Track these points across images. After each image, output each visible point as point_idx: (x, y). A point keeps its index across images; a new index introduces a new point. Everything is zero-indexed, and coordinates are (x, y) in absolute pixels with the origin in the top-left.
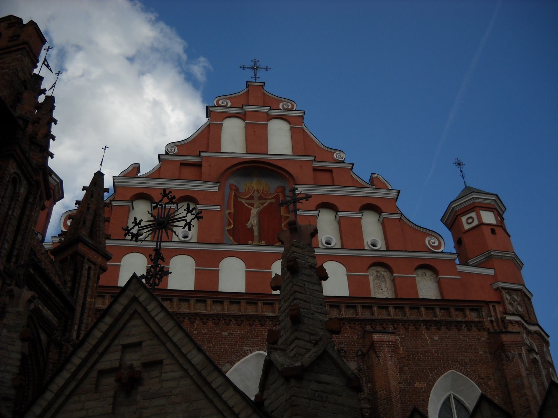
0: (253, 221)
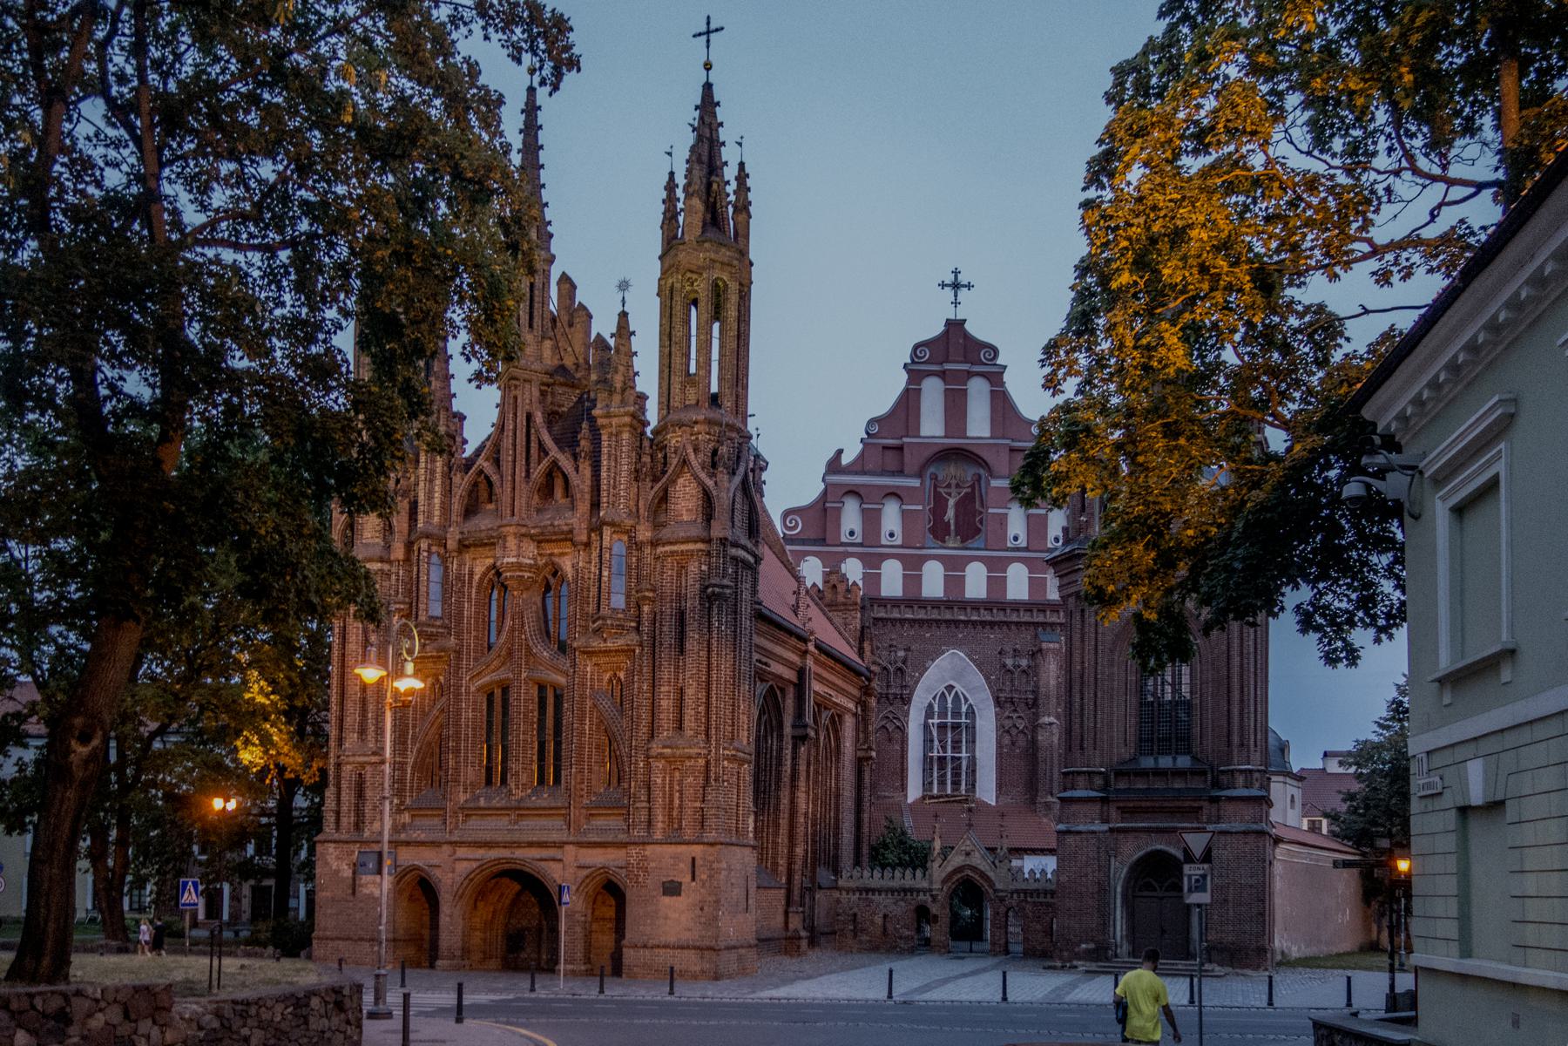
0: (950, 514)
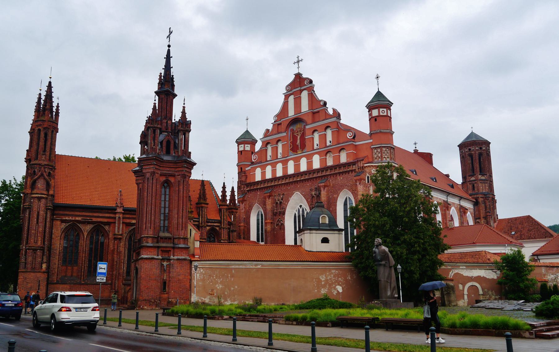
0: (298, 141)
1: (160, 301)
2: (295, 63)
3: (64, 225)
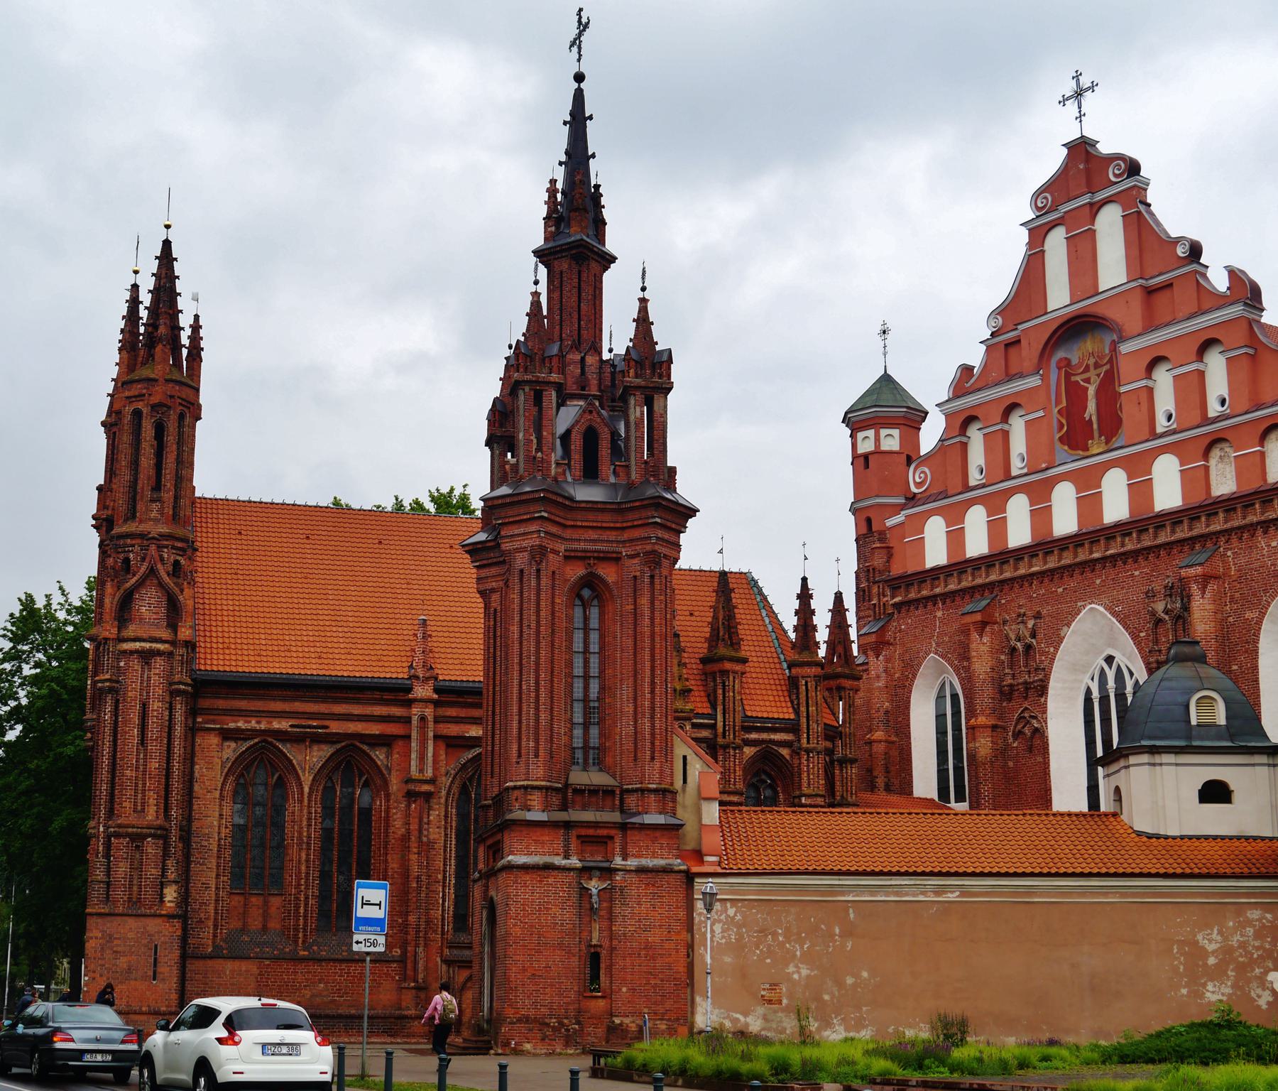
0: (1092, 406)
1: (578, 1023)
2: (1064, 101)
3: (231, 750)
